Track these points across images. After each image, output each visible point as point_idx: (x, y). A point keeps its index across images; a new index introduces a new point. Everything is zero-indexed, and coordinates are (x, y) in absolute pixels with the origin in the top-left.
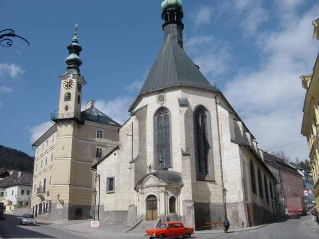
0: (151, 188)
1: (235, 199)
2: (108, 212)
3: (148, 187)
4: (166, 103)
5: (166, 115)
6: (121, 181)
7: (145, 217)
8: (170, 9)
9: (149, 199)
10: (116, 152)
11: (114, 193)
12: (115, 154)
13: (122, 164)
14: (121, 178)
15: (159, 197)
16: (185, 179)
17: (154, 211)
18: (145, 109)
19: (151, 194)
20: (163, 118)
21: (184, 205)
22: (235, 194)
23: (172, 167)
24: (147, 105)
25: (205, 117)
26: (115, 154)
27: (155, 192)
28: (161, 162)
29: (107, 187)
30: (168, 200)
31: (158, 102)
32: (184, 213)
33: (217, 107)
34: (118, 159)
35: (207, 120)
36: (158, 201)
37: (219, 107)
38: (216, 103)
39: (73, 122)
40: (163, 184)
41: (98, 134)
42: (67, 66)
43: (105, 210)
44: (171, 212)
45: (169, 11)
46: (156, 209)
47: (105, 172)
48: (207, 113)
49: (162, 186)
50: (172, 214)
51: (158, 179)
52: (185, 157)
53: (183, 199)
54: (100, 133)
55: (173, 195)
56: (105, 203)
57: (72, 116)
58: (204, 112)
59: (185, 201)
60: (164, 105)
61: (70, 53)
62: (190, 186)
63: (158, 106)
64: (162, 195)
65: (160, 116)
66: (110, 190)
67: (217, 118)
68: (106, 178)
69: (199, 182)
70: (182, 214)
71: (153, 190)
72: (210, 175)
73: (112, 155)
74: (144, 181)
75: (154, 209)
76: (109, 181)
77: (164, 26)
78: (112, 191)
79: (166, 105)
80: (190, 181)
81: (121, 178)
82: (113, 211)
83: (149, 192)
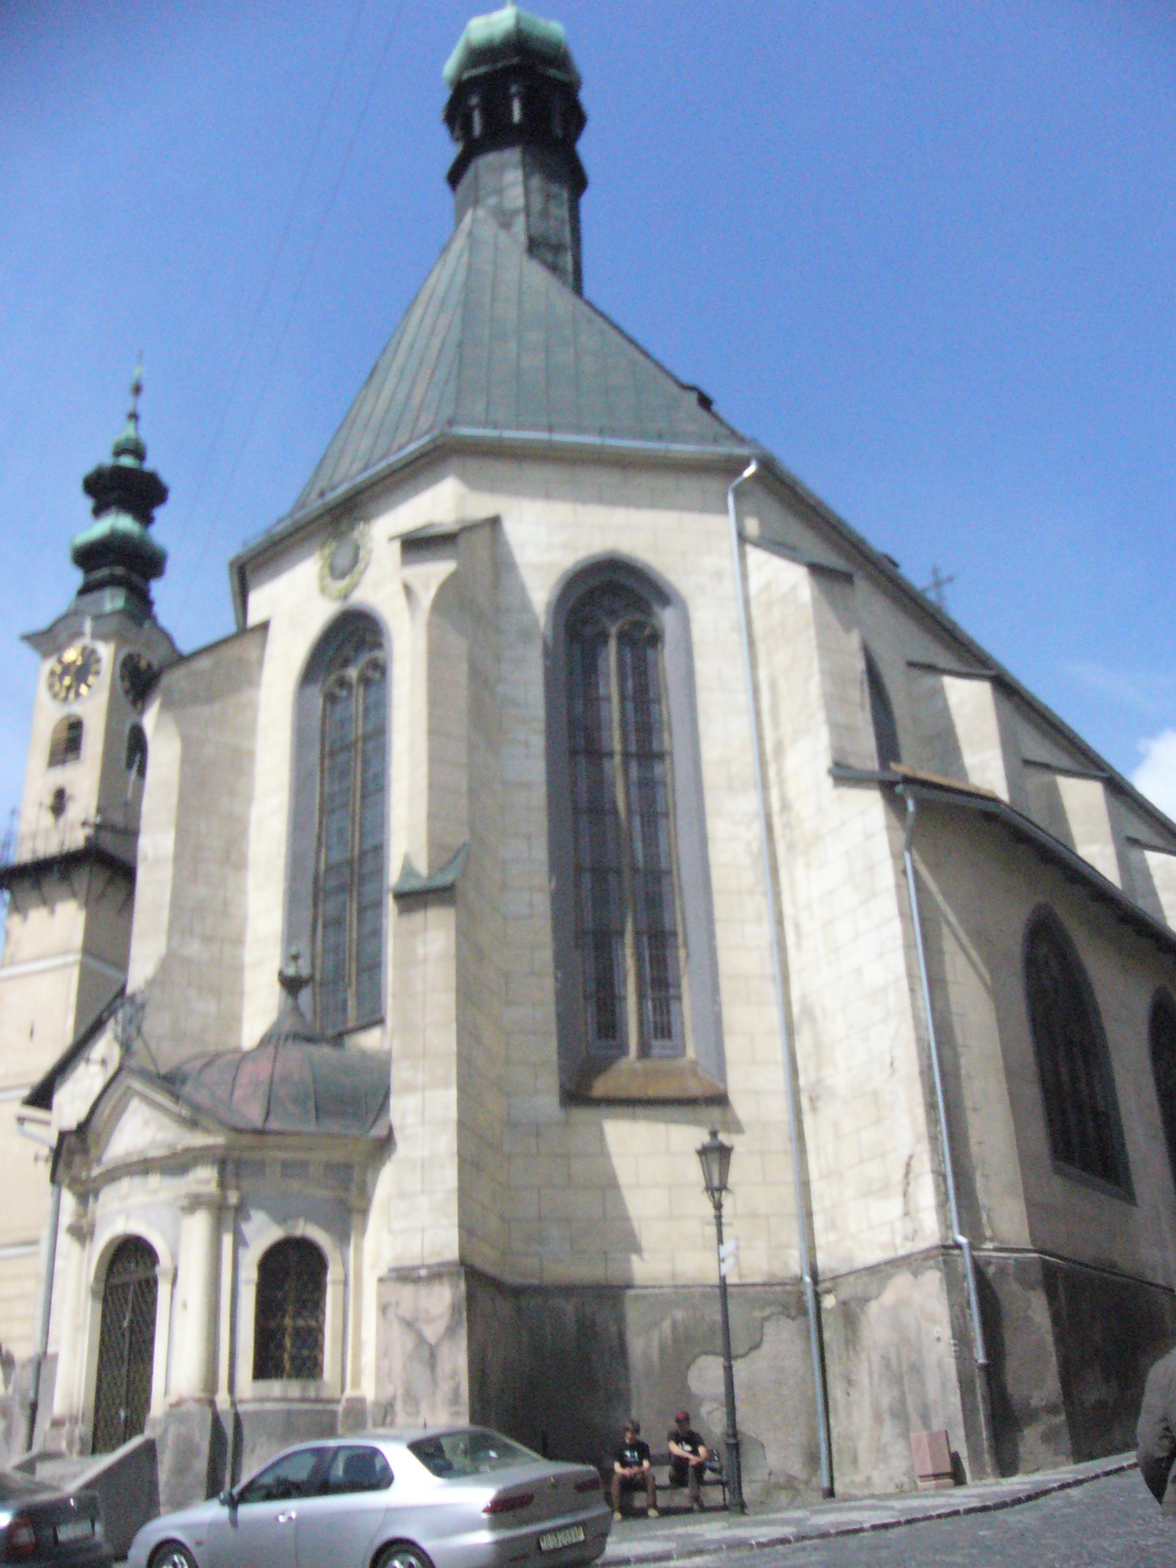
1: (884, 1237)
9: (116, 1281)
15: (174, 1256)
16: (409, 1088)
21: (384, 1309)
22: (881, 1190)
30: (250, 1274)
32: (382, 1377)
33: (742, 556)
35: (669, 658)
36: (163, 1290)
37: (755, 556)
38: (742, 538)
39: (82, 878)
40: (198, 1140)
42: (77, 577)
44: (264, 1368)
48: (667, 618)
50: (276, 1387)
52: (418, 918)
57: (77, 839)
58: (646, 609)
59: (403, 1275)
61: (98, 511)
62: (446, 1143)
64: (198, 1226)
70: (368, 1391)
72: (691, 1053)
77: (455, 176)
80: (446, 1101)
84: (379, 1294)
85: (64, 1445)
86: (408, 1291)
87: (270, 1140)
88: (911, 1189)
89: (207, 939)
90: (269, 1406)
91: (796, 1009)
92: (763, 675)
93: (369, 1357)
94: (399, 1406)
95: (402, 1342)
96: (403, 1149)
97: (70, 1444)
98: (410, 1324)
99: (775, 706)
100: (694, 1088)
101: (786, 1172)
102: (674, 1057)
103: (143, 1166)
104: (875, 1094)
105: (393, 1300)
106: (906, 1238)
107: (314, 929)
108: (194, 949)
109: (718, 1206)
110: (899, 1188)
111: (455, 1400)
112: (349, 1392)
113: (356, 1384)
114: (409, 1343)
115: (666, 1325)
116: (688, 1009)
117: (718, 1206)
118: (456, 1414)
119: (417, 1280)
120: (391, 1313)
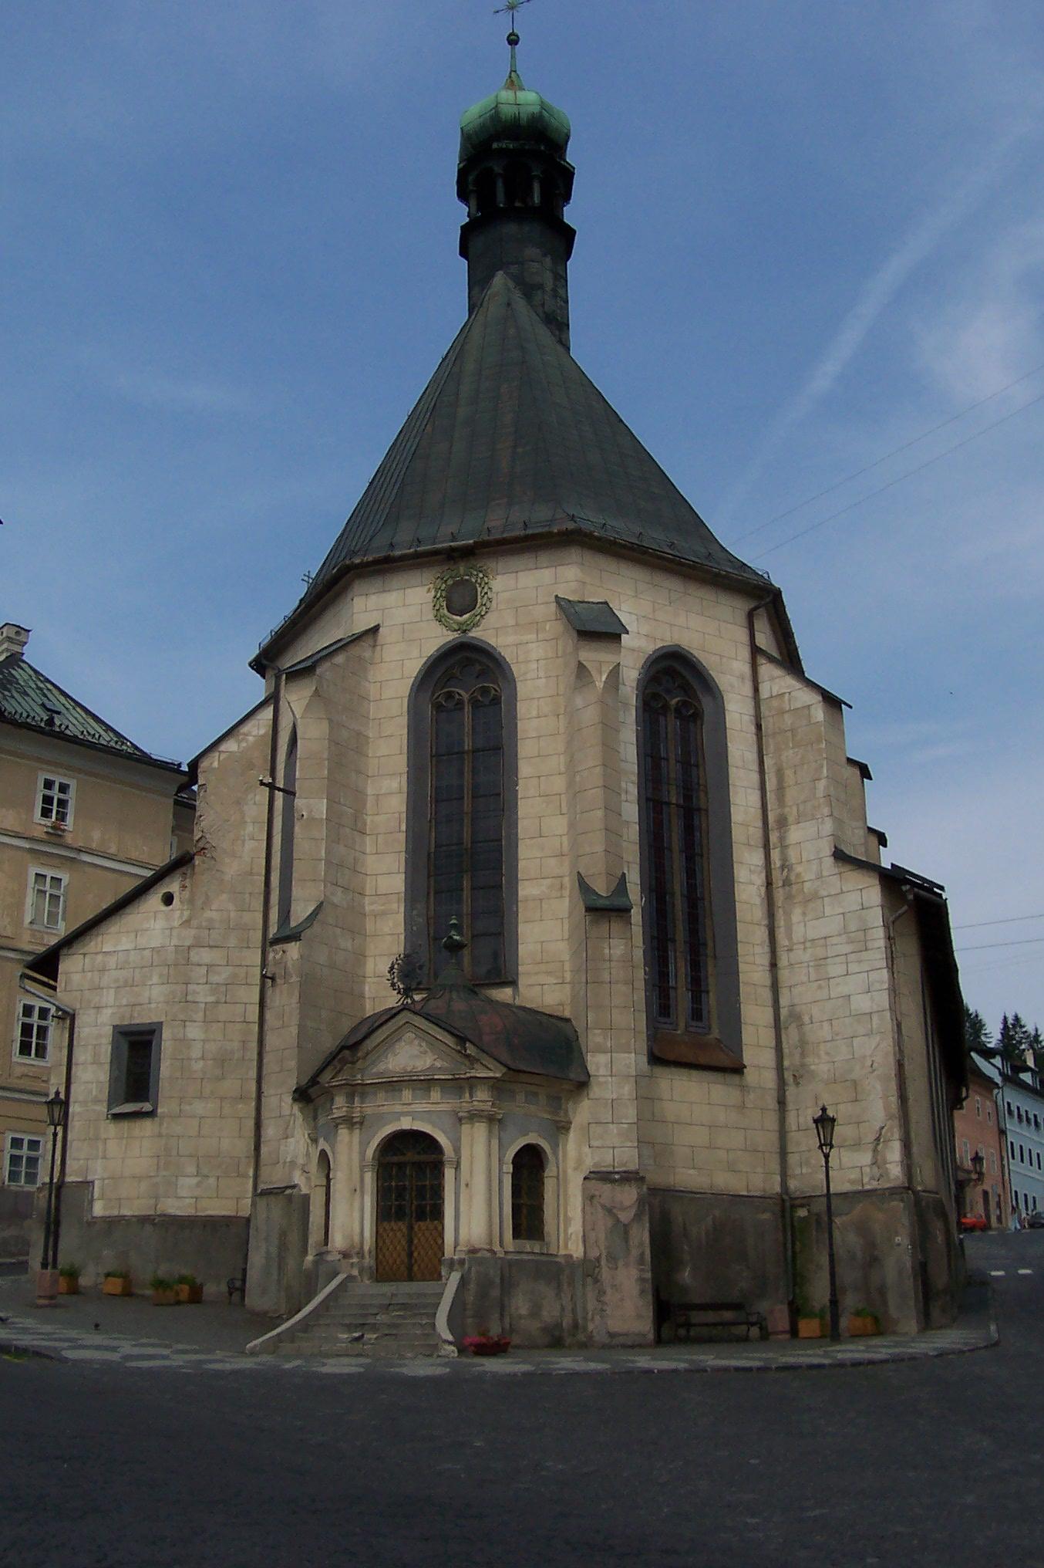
0: (407, 1095)
2: (112, 1223)
3: (394, 1085)
4: (491, 620)
5: (485, 691)
6: (196, 1052)
7: (368, 1261)
8: (505, 144)
10: (173, 886)
11: (151, 1114)
12: (168, 899)
13: (205, 956)
14: (194, 1032)
15: (457, 1150)
16: (600, 1050)
17: (421, 1226)
18: (363, 650)
19: (406, 1124)
20: (467, 708)
21: (589, 1199)
23: (513, 983)
24: (375, 630)
25: (697, 716)
26: (168, 899)
27: (427, 1115)
28: (455, 948)
29: (113, 1080)
31: (439, 619)
34: (187, 923)
36: (449, 1173)
38: (755, 651)
41: (47, 800)
43: (98, 1209)
44: (517, 1234)
45: (501, 152)
46: (438, 1213)
47: (109, 997)
48: (706, 703)
49: (472, 1083)
50: (528, 1245)
51: (449, 1040)
53: (589, 1163)
54: (55, 794)
55: (532, 1139)
56: (98, 1172)
59: (599, 1176)
60: (474, 633)
63: (436, 638)
65: (449, 696)
66: (129, 1099)
67: (759, 727)
68: (108, 1031)
69: (659, 1071)
70: (576, 1250)
71: (420, 1107)
72: (715, 1033)
73: (154, 900)
74: (370, 1044)
75: (421, 1215)
76: (125, 1047)
78: (147, 1107)
79: (488, 632)
81: (194, 1032)
82: (144, 1220)
83: (398, 1116)
84: (584, 1190)
85: (355, 1272)
86: (607, 1187)
87: (523, 1077)
88: (880, 1147)
89: (346, 889)
90: (525, 1257)
91: (784, 1012)
92: (768, 762)
93: (576, 1227)
94: (603, 1262)
95: (603, 1223)
96: (595, 1091)
97: (361, 1272)
98: (609, 1211)
99: (781, 788)
100: (723, 1060)
101: (771, 1122)
102: (709, 1034)
103: (423, 1083)
104: (855, 1082)
105: (597, 1193)
106: (872, 1178)
107: (428, 893)
108: (338, 897)
109: (827, 1156)
110: (871, 1146)
111: (641, 1261)
112: (562, 1252)
113: (566, 1246)
114: (610, 1222)
115: (709, 1219)
116: (712, 1000)
117: (827, 1156)
118: (642, 1270)
119: (614, 1181)
120: (595, 1201)
